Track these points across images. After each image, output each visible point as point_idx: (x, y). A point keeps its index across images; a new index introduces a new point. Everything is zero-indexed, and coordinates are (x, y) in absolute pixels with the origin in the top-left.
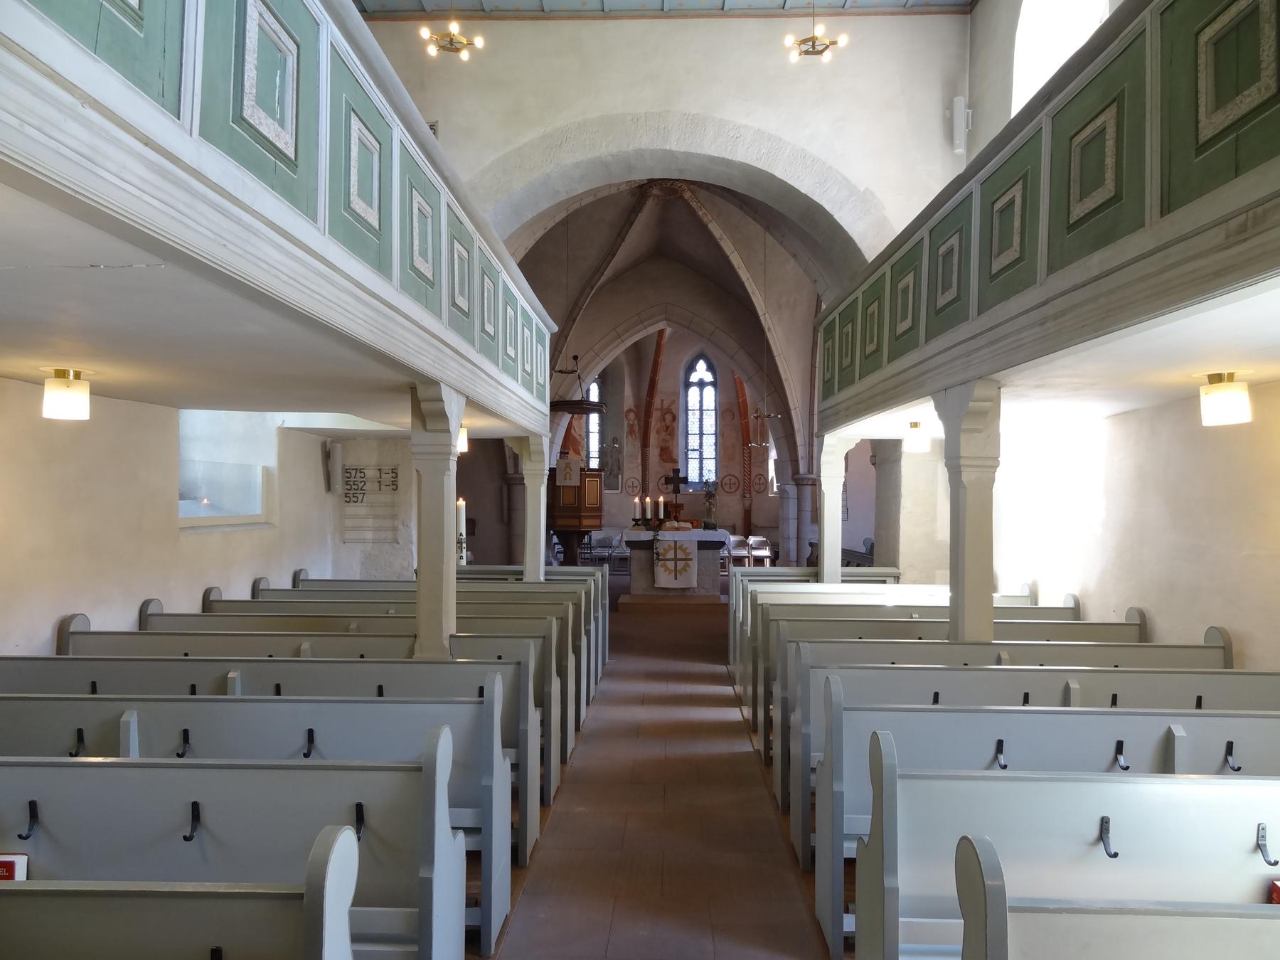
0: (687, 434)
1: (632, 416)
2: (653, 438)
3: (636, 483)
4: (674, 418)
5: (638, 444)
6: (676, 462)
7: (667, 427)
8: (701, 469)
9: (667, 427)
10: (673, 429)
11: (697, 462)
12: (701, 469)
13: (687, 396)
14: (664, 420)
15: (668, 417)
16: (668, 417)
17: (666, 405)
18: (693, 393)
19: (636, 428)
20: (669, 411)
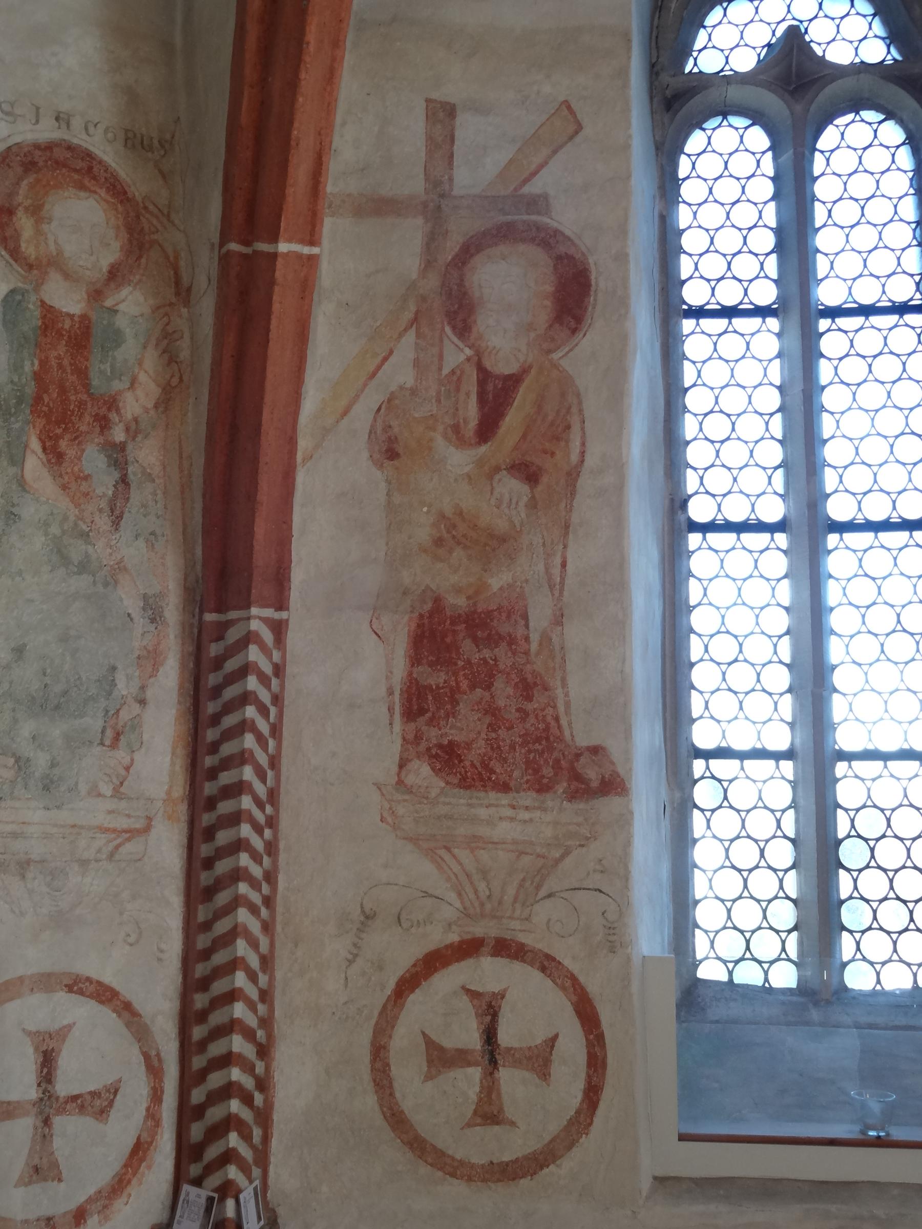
0: (677, 525)
1: (79, 227)
2: (333, 517)
3: (96, 1052)
4: (572, 295)
5: (150, 562)
6: (591, 780)
7: (497, 396)
8: (820, 854)
9: (497, 396)
10: (558, 424)
11: (777, 785)
12: (820, 854)
13: (668, 187)
14: (460, 311)
15: (509, 286)
16: (509, 286)
17: (481, 162)
18: (727, 162)
19: (132, 376)
20: (517, 223)
